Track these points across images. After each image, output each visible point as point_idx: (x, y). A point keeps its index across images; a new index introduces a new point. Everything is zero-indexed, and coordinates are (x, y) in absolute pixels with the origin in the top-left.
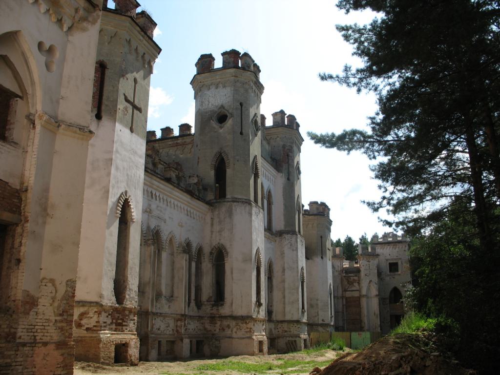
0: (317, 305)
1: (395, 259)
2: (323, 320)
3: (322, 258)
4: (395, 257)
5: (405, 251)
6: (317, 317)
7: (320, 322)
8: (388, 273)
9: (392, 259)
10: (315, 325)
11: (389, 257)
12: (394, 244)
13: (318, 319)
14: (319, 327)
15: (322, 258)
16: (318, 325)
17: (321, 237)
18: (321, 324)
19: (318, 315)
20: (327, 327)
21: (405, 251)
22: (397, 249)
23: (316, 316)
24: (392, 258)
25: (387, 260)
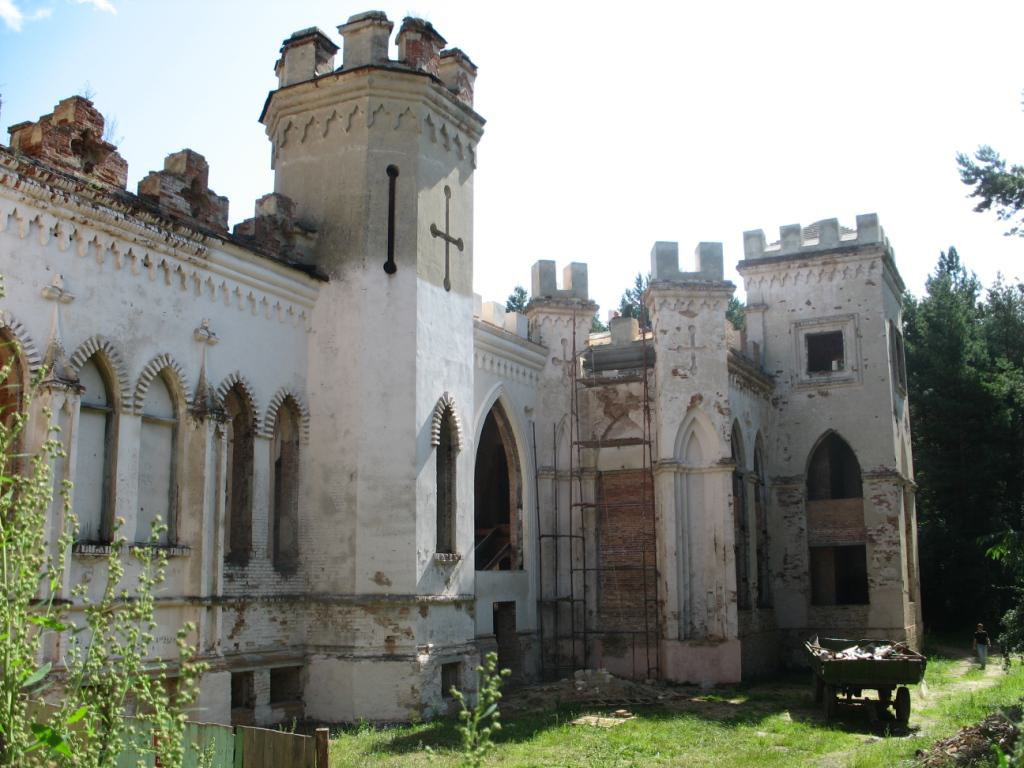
0: (351, 500)
1: (829, 320)
2: (379, 578)
3: (390, 268)
4: (831, 312)
5: (870, 283)
6: (349, 562)
7: (365, 586)
8: (805, 377)
9: (819, 321)
10: (339, 603)
11: (804, 313)
12: (827, 258)
13: (353, 571)
14: (359, 612)
15: (390, 268)
16: (351, 602)
17: (393, 172)
18: (366, 597)
19: (353, 552)
20: (405, 610)
21: (870, 283)
22: (838, 279)
23: (343, 558)
24: (818, 314)
25: (798, 325)
